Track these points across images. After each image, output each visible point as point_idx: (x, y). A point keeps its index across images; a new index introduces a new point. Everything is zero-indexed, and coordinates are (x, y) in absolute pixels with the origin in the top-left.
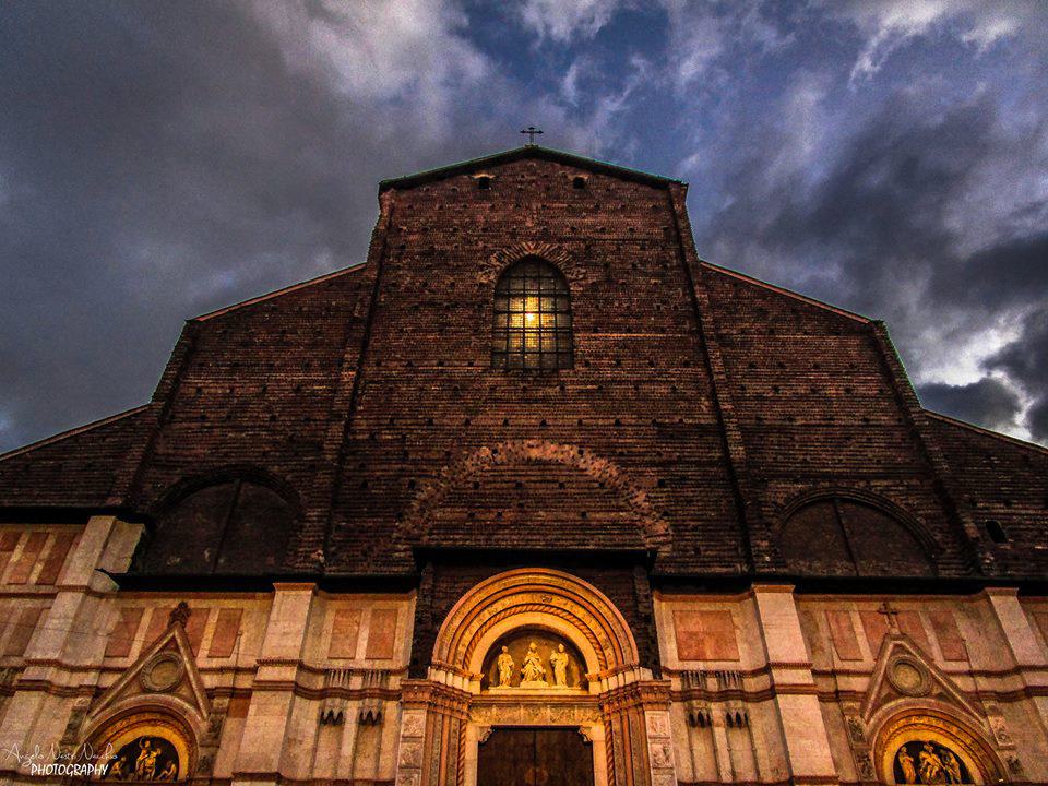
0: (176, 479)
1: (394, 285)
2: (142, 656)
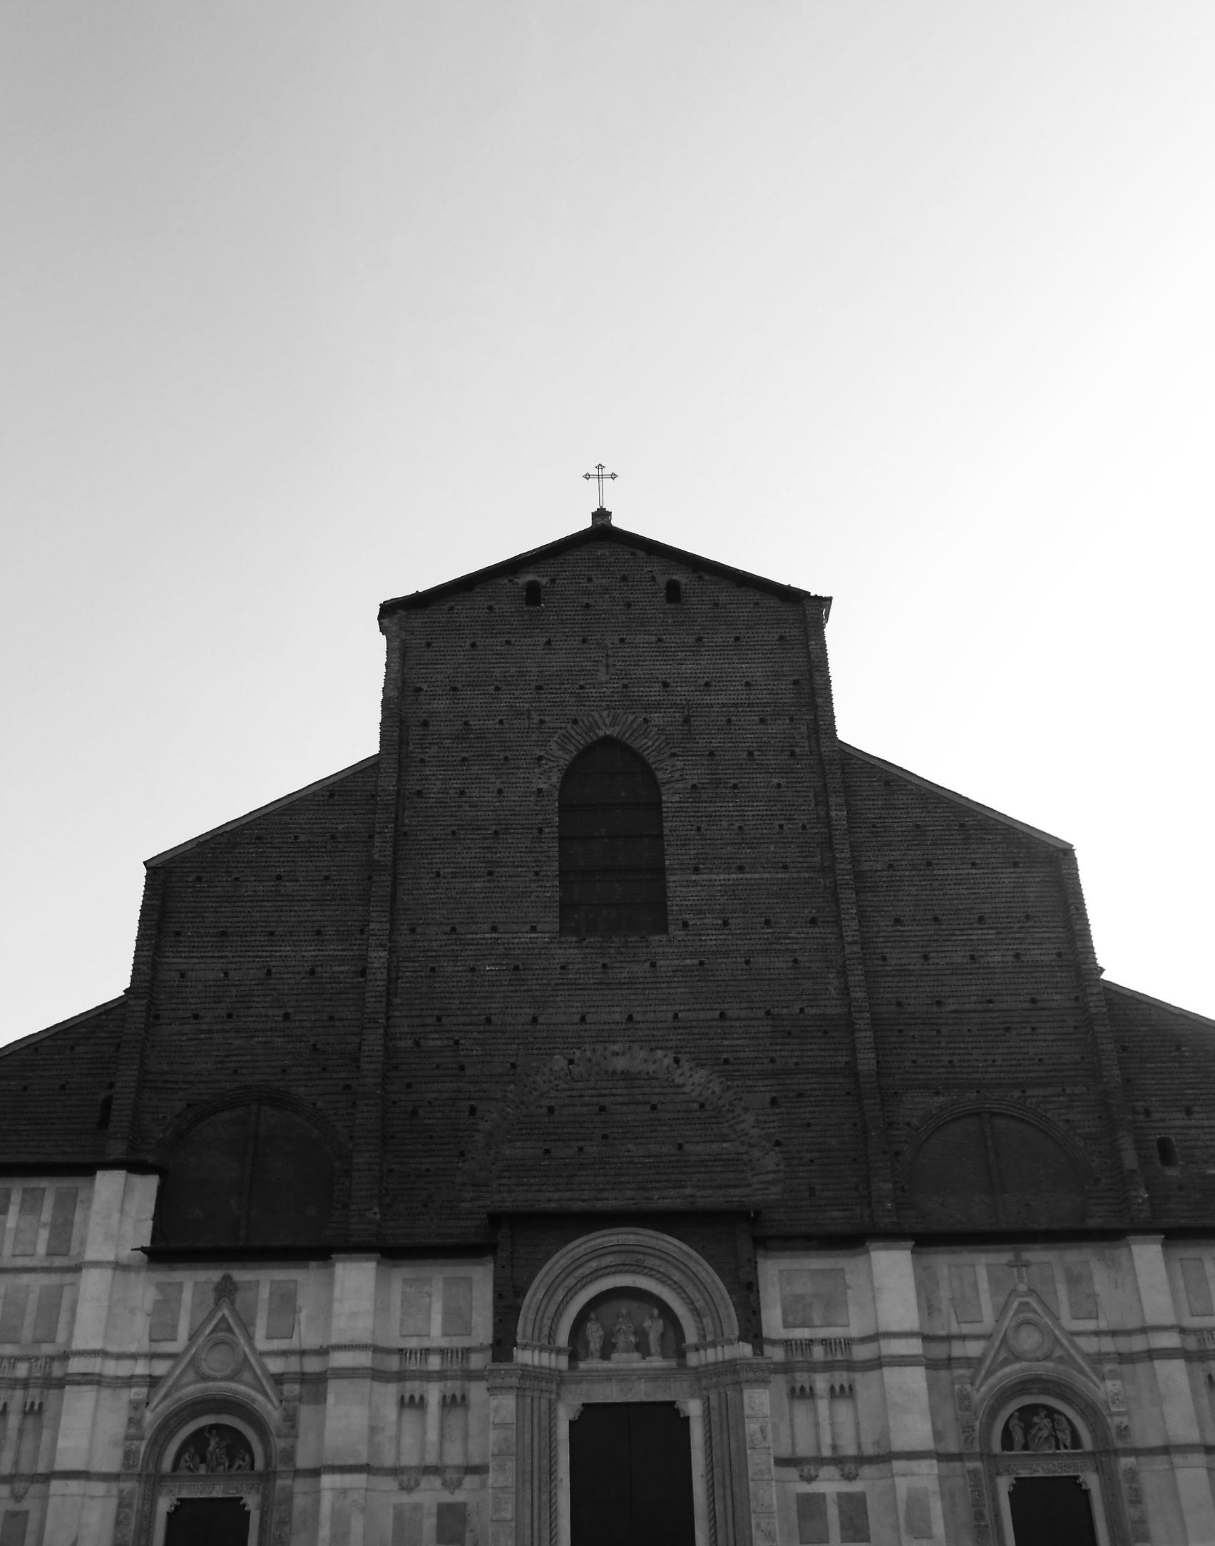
1: (419, 793)
2: (192, 1338)
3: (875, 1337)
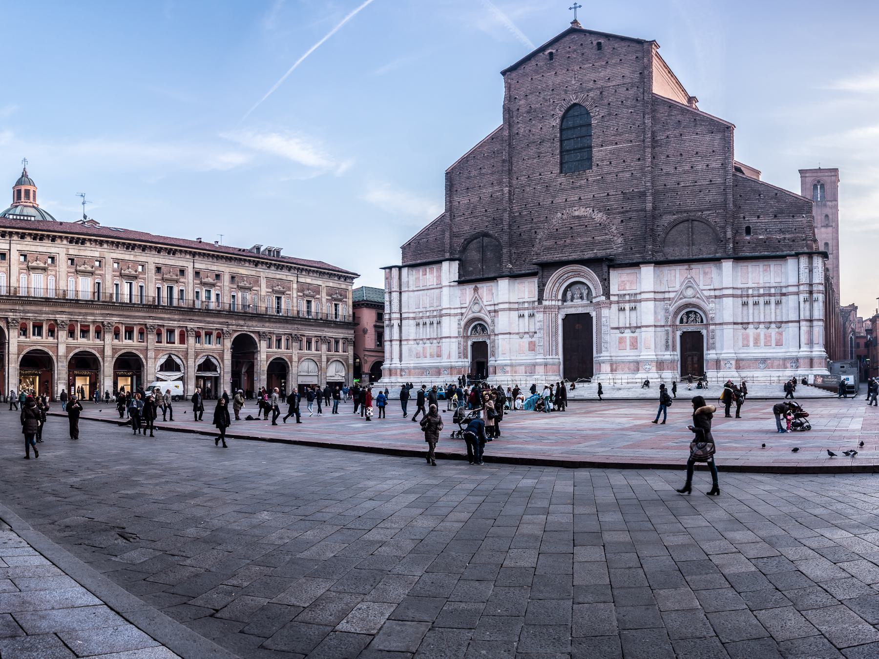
0: (463, 240)
2: (470, 303)
3: (640, 293)
